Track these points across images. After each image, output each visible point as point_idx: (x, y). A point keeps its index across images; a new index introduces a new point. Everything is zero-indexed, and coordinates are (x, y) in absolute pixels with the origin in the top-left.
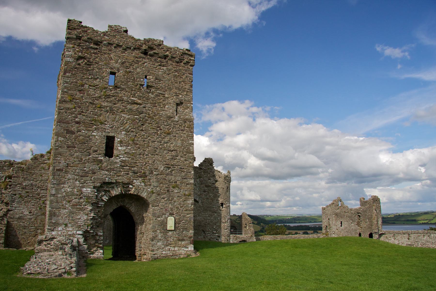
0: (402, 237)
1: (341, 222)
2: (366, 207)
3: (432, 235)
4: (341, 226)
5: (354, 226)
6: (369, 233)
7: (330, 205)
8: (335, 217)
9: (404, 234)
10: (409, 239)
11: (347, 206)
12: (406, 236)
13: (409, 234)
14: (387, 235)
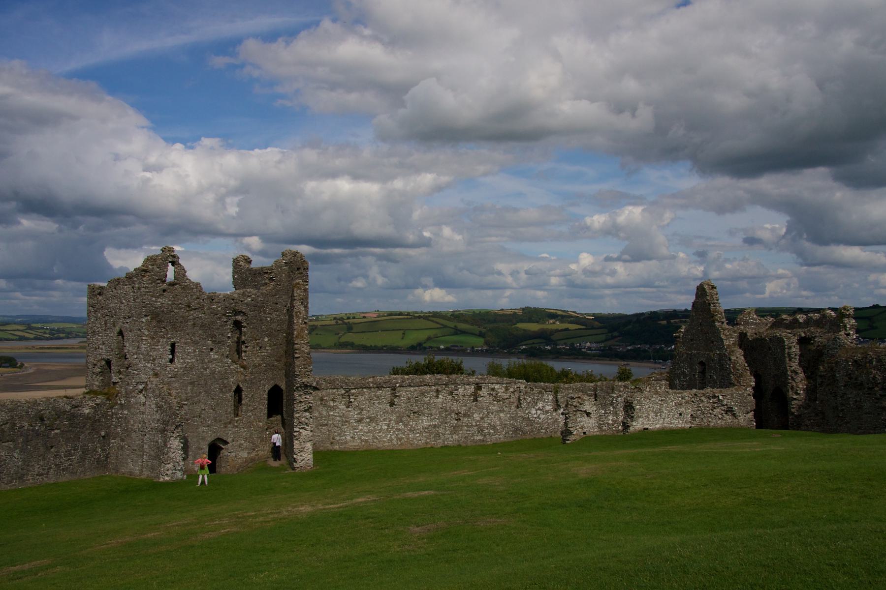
0: (370, 398)
1: (173, 345)
2: (264, 290)
3: (461, 390)
4: (172, 361)
5: (218, 360)
6: (267, 388)
7: (129, 277)
8: (149, 323)
9: (379, 387)
10: (392, 404)
11: (198, 285)
12: (386, 393)
13: (394, 389)
14: (324, 392)
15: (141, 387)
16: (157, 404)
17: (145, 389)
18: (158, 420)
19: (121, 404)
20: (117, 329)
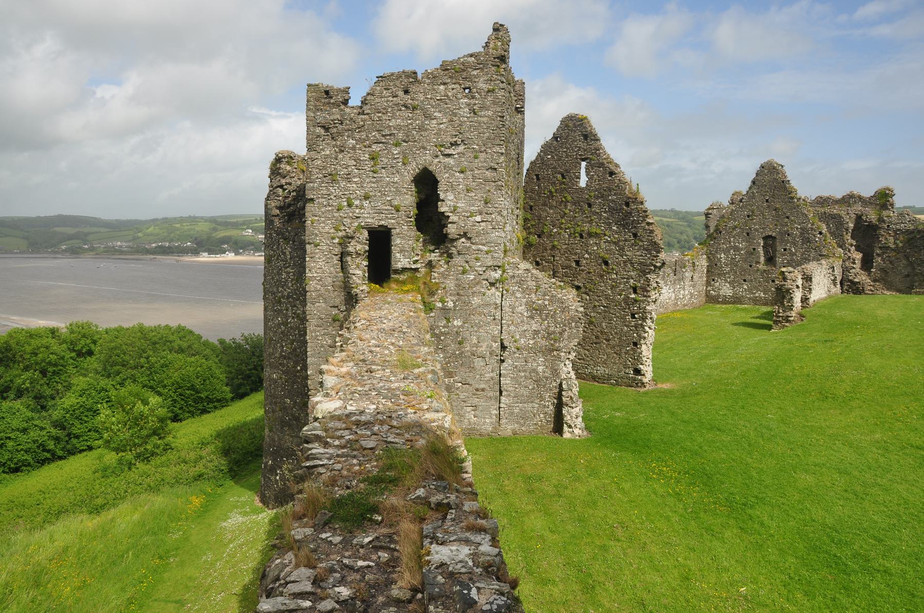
15: (497, 275)
16: (530, 306)
17: (501, 281)
18: (536, 332)
19: (444, 309)
20: (413, 169)
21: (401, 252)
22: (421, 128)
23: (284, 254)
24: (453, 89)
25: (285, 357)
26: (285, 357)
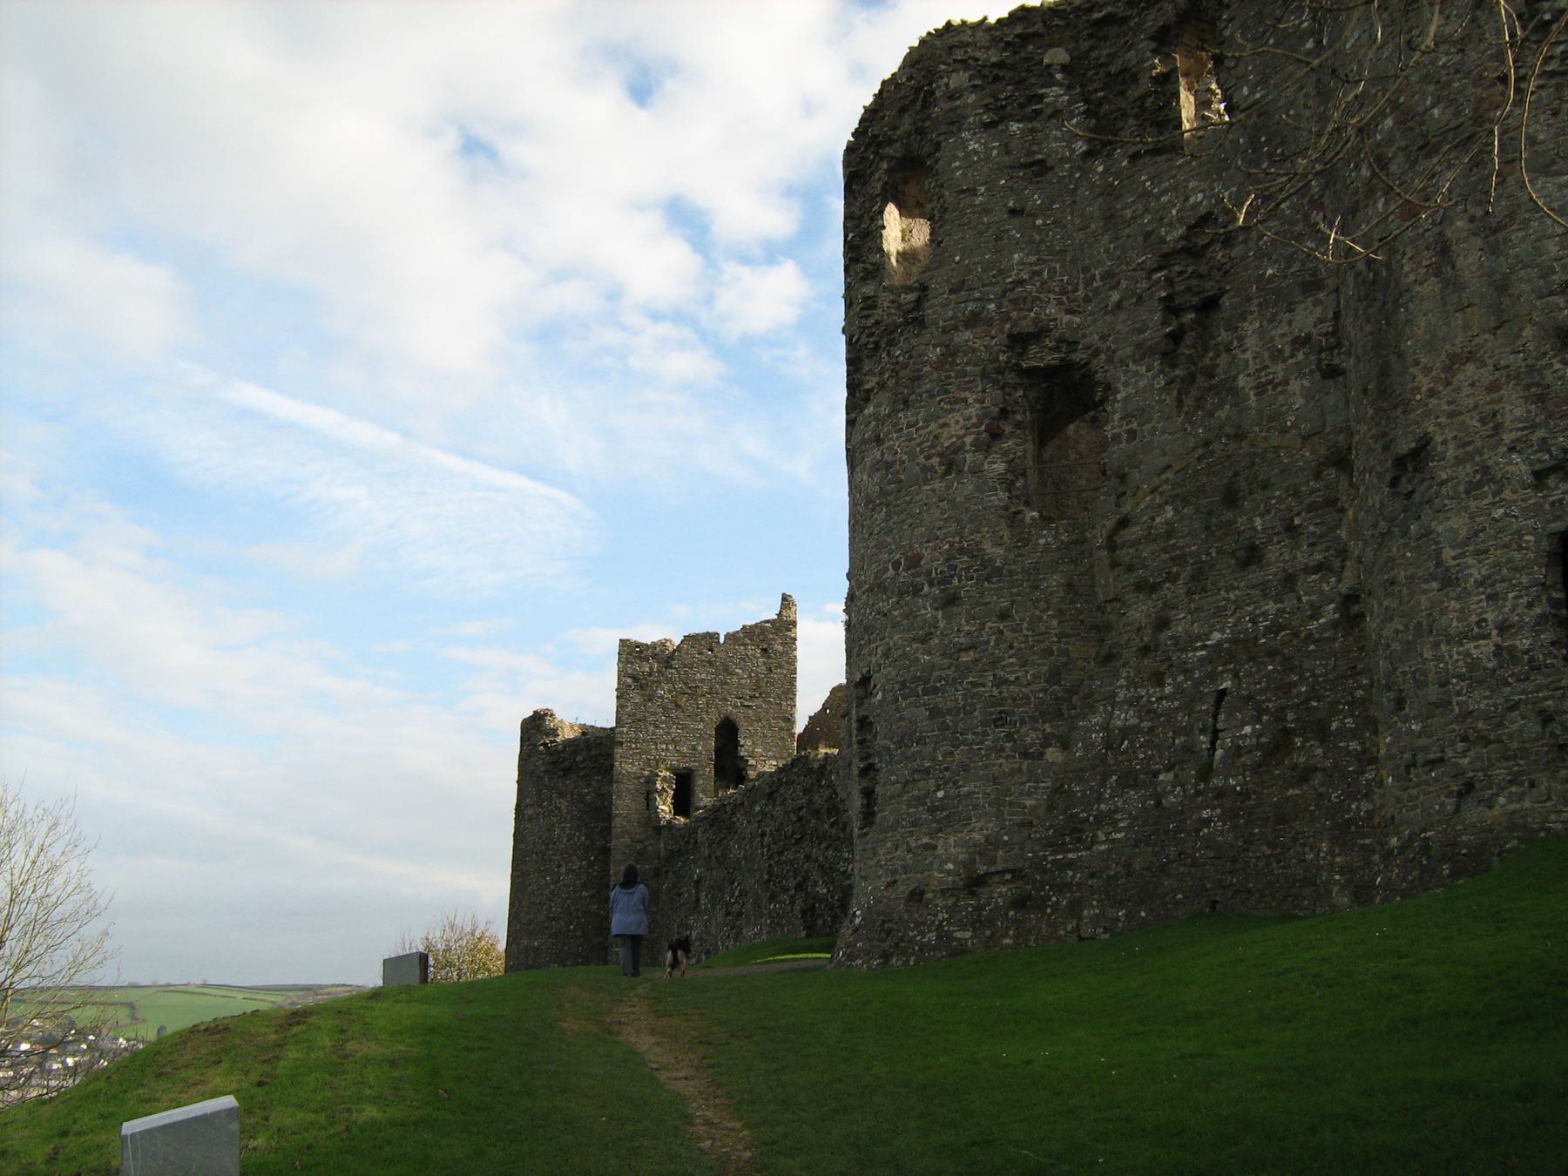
20: (714, 718)
21: (704, 792)
22: (723, 683)
23: (559, 809)
24: (753, 650)
25: (553, 919)
26: (553, 919)
